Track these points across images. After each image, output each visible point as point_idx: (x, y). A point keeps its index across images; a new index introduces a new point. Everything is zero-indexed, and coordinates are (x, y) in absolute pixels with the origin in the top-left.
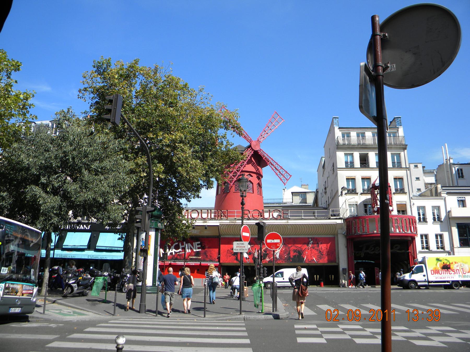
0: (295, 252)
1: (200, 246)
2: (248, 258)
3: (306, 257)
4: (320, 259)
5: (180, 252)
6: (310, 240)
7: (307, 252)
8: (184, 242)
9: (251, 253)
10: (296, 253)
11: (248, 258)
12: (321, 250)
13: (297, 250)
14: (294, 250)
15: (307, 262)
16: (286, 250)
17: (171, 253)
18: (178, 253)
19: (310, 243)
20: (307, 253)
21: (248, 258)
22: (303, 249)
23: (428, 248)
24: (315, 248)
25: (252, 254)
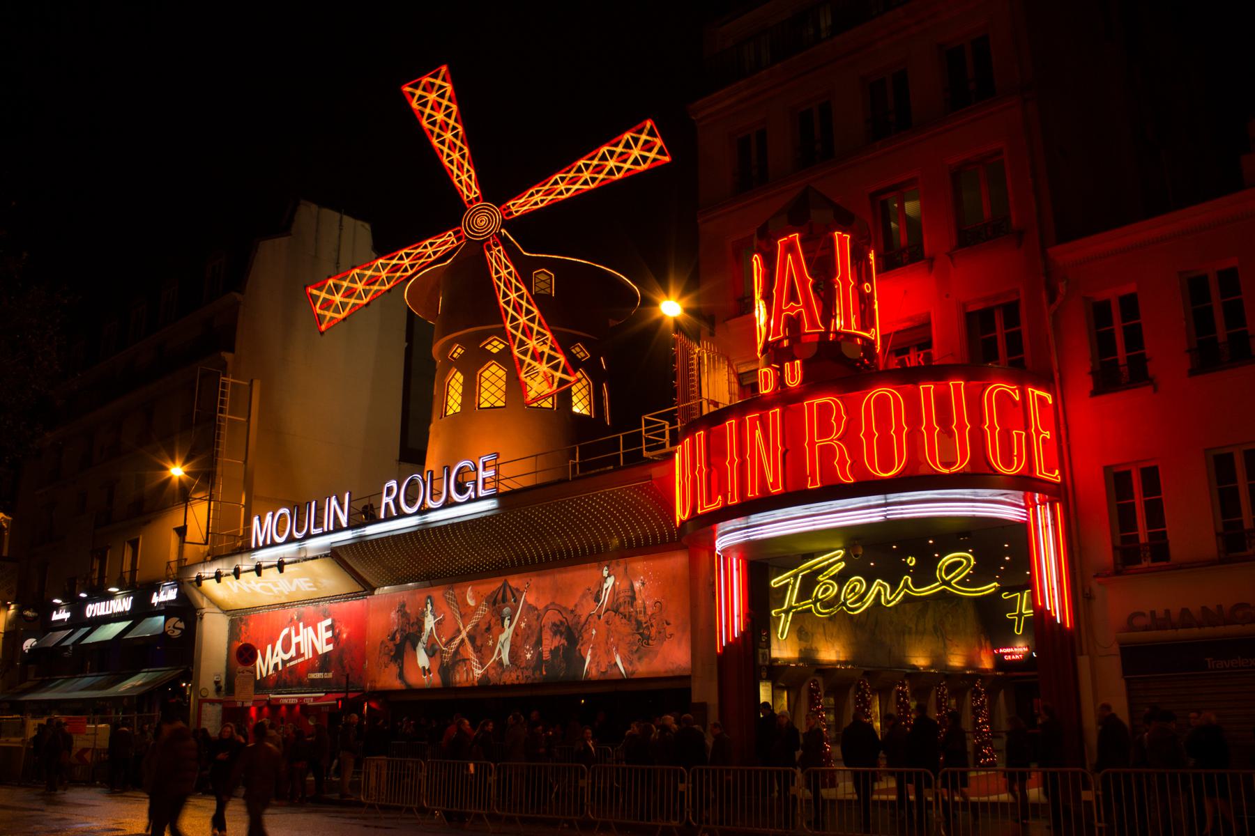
0: (555, 634)
1: (330, 634)
2: (427, 668)
3: (590, 652)
4: (639, 659)
5: (291, 659)
6: (605, 573)
7: (594, 632)
8: (301, 625)
9: (437, 647)
10: (558, 637)
11: (429, 671)
12: (641, 618)
13: (561, 622)
14: (554, 624)
15: (594, 673)
16: (529, 626)
17: (276, 665)
18: (288, 665)
19: (605, 586)
20: (596, 634)
21: (427, 668)
22: (583, 619)
23: (1159, 549)
24: (622, 609)
25: (438, 655)
